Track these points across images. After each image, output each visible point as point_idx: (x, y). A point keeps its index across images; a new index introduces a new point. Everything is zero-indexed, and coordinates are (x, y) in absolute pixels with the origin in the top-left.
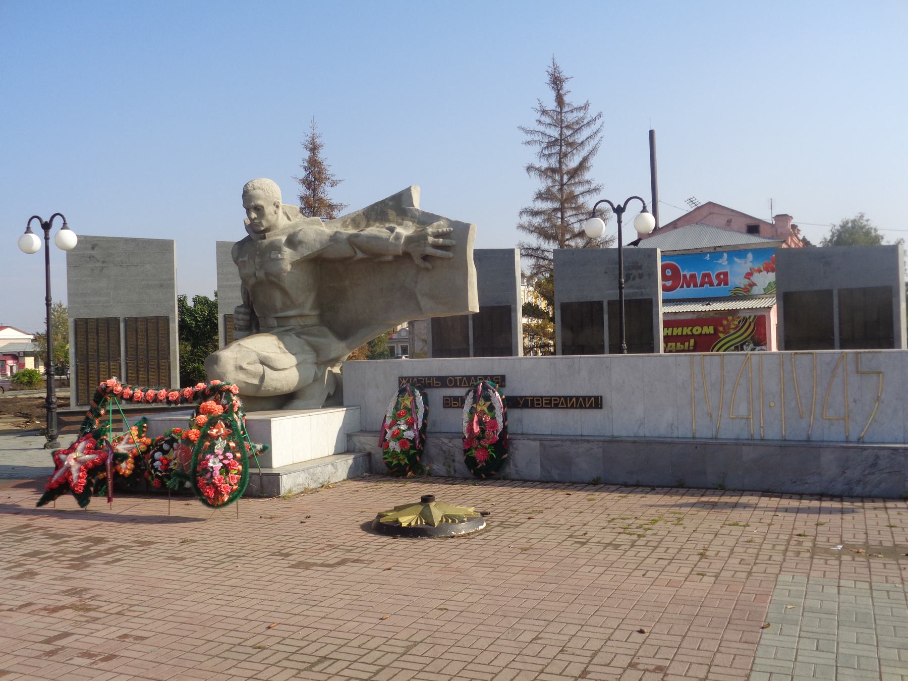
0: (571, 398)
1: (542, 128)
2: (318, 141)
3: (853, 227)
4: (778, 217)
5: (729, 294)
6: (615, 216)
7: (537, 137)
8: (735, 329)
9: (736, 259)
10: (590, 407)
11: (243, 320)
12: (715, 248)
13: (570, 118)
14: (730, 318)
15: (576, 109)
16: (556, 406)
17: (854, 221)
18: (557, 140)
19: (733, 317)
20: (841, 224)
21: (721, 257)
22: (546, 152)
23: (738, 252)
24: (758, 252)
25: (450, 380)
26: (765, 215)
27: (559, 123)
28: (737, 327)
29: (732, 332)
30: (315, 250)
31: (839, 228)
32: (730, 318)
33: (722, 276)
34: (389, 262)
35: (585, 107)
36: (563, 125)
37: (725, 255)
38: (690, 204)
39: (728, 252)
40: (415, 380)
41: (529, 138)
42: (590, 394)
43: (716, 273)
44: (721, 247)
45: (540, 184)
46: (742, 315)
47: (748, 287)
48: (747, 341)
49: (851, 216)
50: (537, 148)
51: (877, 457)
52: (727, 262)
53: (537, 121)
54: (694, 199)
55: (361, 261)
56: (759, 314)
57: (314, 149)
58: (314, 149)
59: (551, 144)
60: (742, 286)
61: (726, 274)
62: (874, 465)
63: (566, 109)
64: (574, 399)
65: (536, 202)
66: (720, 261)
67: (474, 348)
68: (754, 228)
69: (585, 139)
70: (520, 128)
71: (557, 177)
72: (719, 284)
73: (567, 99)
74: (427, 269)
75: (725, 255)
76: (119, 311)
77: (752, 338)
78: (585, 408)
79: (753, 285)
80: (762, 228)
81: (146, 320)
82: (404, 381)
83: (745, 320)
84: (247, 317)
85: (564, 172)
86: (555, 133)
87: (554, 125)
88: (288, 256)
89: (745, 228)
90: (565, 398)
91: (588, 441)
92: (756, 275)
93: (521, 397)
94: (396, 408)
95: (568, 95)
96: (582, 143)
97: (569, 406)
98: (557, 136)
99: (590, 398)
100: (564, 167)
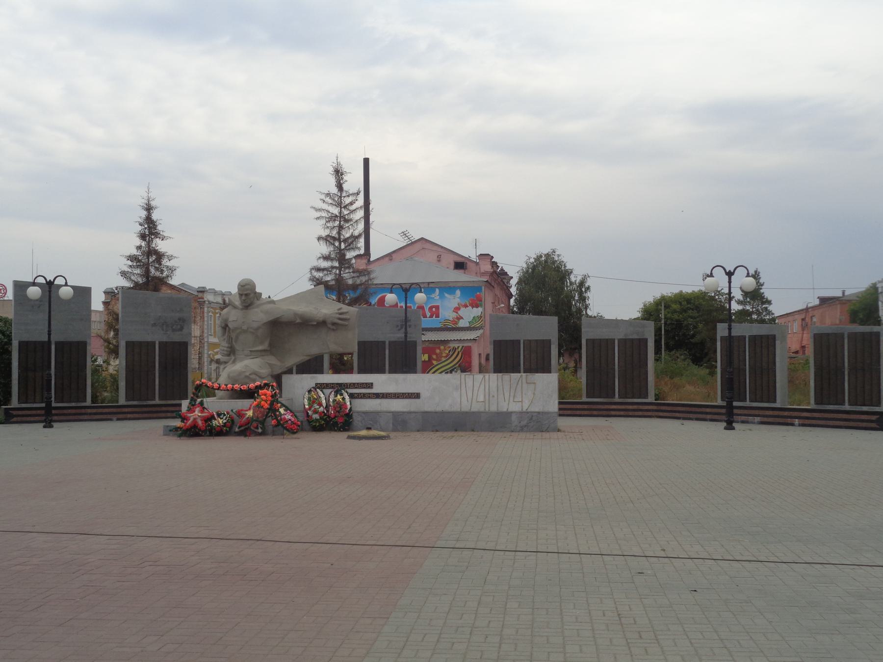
0: (405, 393)
1: (325, 206)
2: (153, 203)
3: (546, 261)
4: (482, 256)
5: (440, 326)
6: (404, 293)
7: (324, 214)
8: (446, 356)
9: (446, 295)
10: (415, 398)
11: (226, 351)
12: (429, 283)
13: (347, 200)
14: (442, 347)
15: (352, 194)
16: (398, 398)
17: (547, 255)
18: (336, 216)
19: (445, 347)
20: (535, 256)
21: (434, 291)
22: (328, 225)
23: (447, 288)
24: (466, 289)
25: (344, 385)
26: (469, 252)
27: (339, 204)
28: (448, 355)
29: (443, 359)
30: (275, 317)
31: (533, 261)
32: (442, 347)
33: (434, 309)
34: (313, 325)
36: (342, 206)
37: (437, 290)
38: (404, 237)
39: (440, 288)
40: (325, 385)
41: (318, 214)
42: (414, 392)
43: (429, 306)
44: (433, 282)
45: (325, 249)
46: (452, 345)
47: (456, 320)
48: (455, 368)
50: (323, 221)
51: (532, 416)
52: (438, 297)
53: (321, 200)
54: (407, 232)
55: (299, 324)
56: (466, 345)
57: (149, 208)
58: (149, 208)
59: (333, 218)
60: (451, 319)
61: (437, 307)
62: (531, 419)
63: (344, 194)
64: (407, 394)
65: (319, 261)
66: (433, 296)
67: (296, 369)
68: (460, 265)
69: (358, 219)
70: (312, 207)
71: (337, 244)
72: (431, 316)
73: (345, 187)
74: (333, 330)
75: (437, 290)
77: (459, 366)
78: (412, 398)
79: (462, 318)
80: (469, 264)
81: (70, 344)
82: (318, 385)
83: (455, 349)
84: (229, 349)
85: (342, 240)
86: (335, 211)
87: (335, 205)
89: (452, 266)
90: (403, 393)
91: (415, 412)
92: (463, 309)
93: (381, 393)
94: (309, 399)
95: (346, 183)
96: (357, 221)
97: (405, 397)
98: (338, 214)
99: (414, 393)
100: (342, 237)
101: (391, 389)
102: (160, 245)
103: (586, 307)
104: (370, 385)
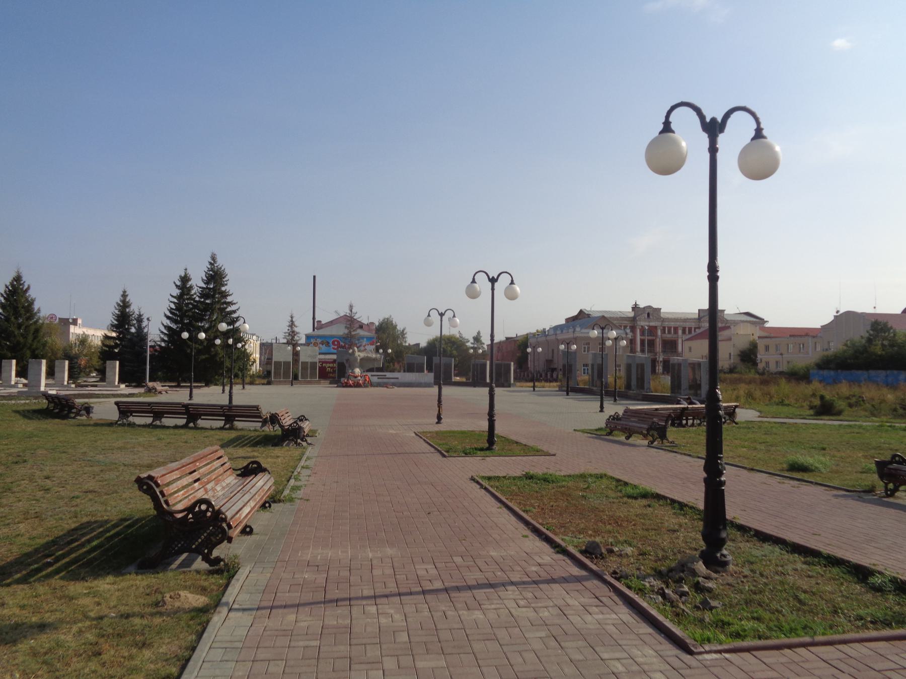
17: (388, 319)
35: (356, 313)
49: (387, 317)
57: (292, 317)
58: (292, 317)
73: (353, 311)
76: (282, 360)
88: (359, 358)
101: (391, 376)
102: (296, 329)
103: (406, 342)
104: (385, 376)
